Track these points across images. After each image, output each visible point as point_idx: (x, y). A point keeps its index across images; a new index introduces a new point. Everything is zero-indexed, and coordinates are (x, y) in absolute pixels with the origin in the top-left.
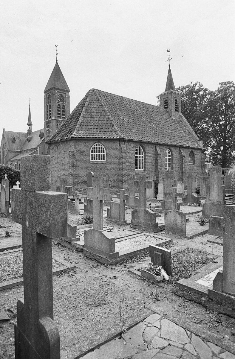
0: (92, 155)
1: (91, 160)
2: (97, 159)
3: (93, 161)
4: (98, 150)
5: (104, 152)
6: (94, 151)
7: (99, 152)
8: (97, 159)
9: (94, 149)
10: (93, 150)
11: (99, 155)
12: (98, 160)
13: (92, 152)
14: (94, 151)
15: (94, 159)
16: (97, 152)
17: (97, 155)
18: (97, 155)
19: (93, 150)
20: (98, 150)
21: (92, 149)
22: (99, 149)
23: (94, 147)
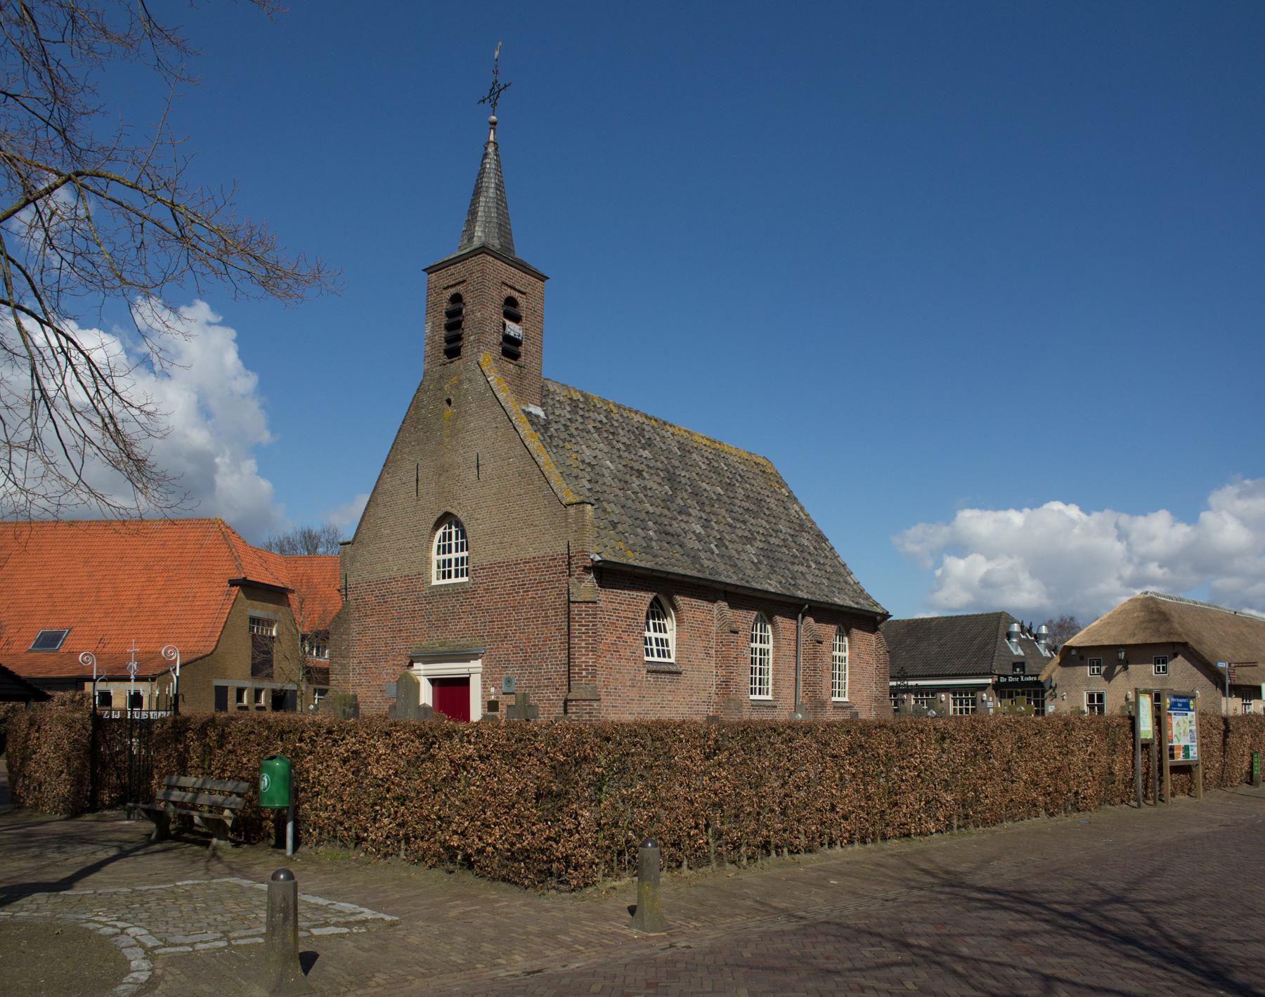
1: (435, 582)
21: (440, 542)
23: (444, 534)
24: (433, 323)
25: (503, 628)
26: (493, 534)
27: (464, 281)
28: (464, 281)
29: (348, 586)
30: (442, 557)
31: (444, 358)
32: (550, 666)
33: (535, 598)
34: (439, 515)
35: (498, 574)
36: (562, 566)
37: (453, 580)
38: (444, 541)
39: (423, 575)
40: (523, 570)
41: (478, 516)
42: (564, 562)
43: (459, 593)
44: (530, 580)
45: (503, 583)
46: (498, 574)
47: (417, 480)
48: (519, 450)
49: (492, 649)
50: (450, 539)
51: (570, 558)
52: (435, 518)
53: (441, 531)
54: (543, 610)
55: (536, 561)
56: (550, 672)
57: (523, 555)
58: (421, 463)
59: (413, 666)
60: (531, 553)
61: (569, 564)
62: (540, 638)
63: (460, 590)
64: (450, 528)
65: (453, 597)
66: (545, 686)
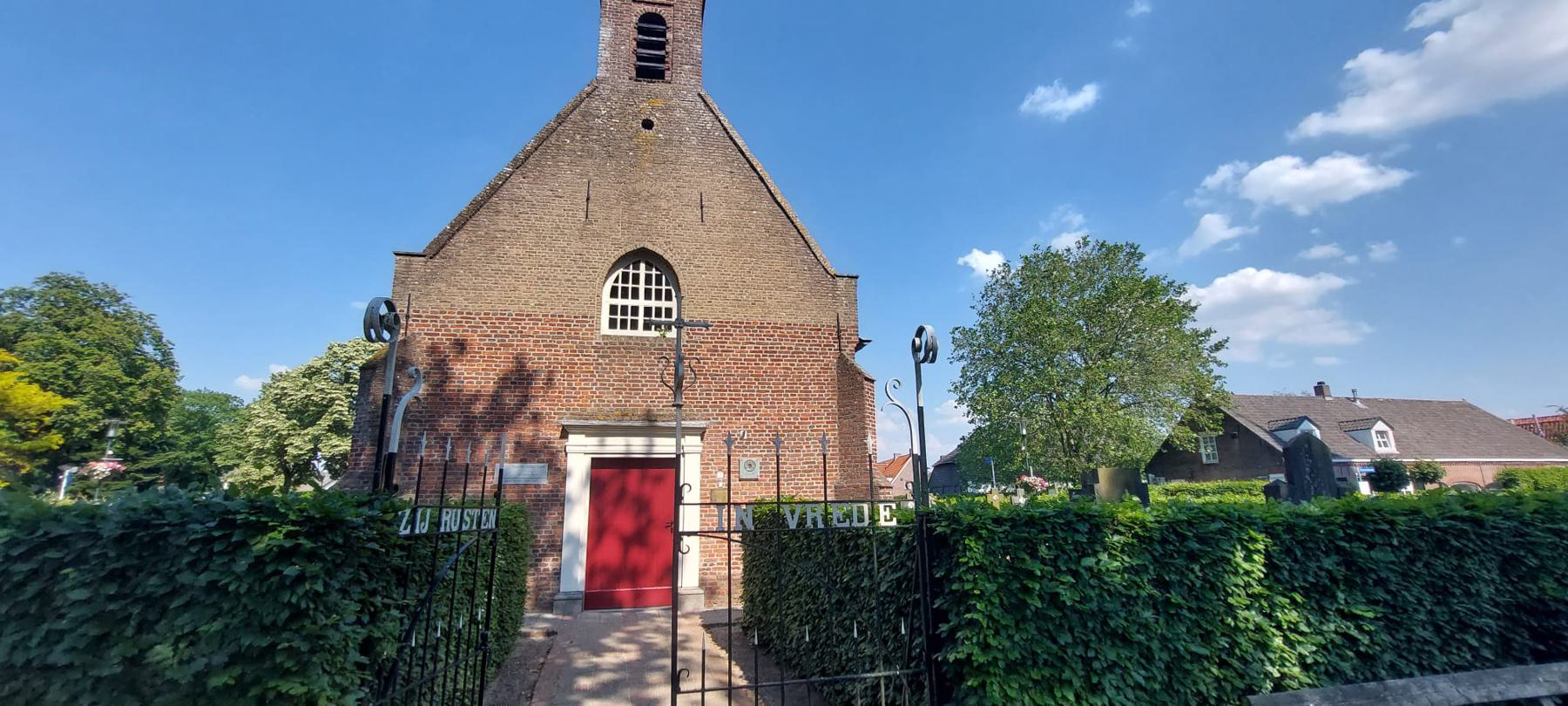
0: (613, 309)
2: (634, 325)
3: (618, 332)
4: (642, 286)
5: (669, 298)
6: (625, 290)
7: (648, 295)
8: (634, 325)
9: (625, 280)
10: (620, 285)
11: (648, 311)
12: (640, 332)
13: (614, 293)
14: (625, 290)
15: (624, 324)
16: (635, 295)
17: (635, 310)
18: (635, 310)
19: (620, 285)
20: (642, 286)
21: (616, 281)
22: (648, 279)
24: (615, 29)
25: (740, 399)
26: (725, 287)
27: (670, 5)
28: (670, 5)
29: (411, 313)
30: (619, 302)
31: (634, 74)
32: (812, 448)
33: (790, 369)
34: (629, 250)
35: (731, 335)
36: (828, 338)
37: (640, 332)
38: (625, 280)
39: (589, 319)
40: (772, 336)
41: (700, 263)
42: (831, 334)
43: (666, 350)
44: (782, 348)
45: (740, 346)
46: (731, 335)
47: (588, 199)
48: (767, 203)
49: (720, 423)
50: (636, 279)
51: (839, 331)
52: (622, 252)
53: (619, 272)
54: (803, 384)
55: (792, 328)
56: (812, 455)
57: (772, 319)
58: (596, 180)
59: (567, 438)
60: (783, 317)
61: (839, 338)
62: (798, 415)
63: (665, 346)
64: (636, 267)
65: (651, 354)
66: (805, 471)
